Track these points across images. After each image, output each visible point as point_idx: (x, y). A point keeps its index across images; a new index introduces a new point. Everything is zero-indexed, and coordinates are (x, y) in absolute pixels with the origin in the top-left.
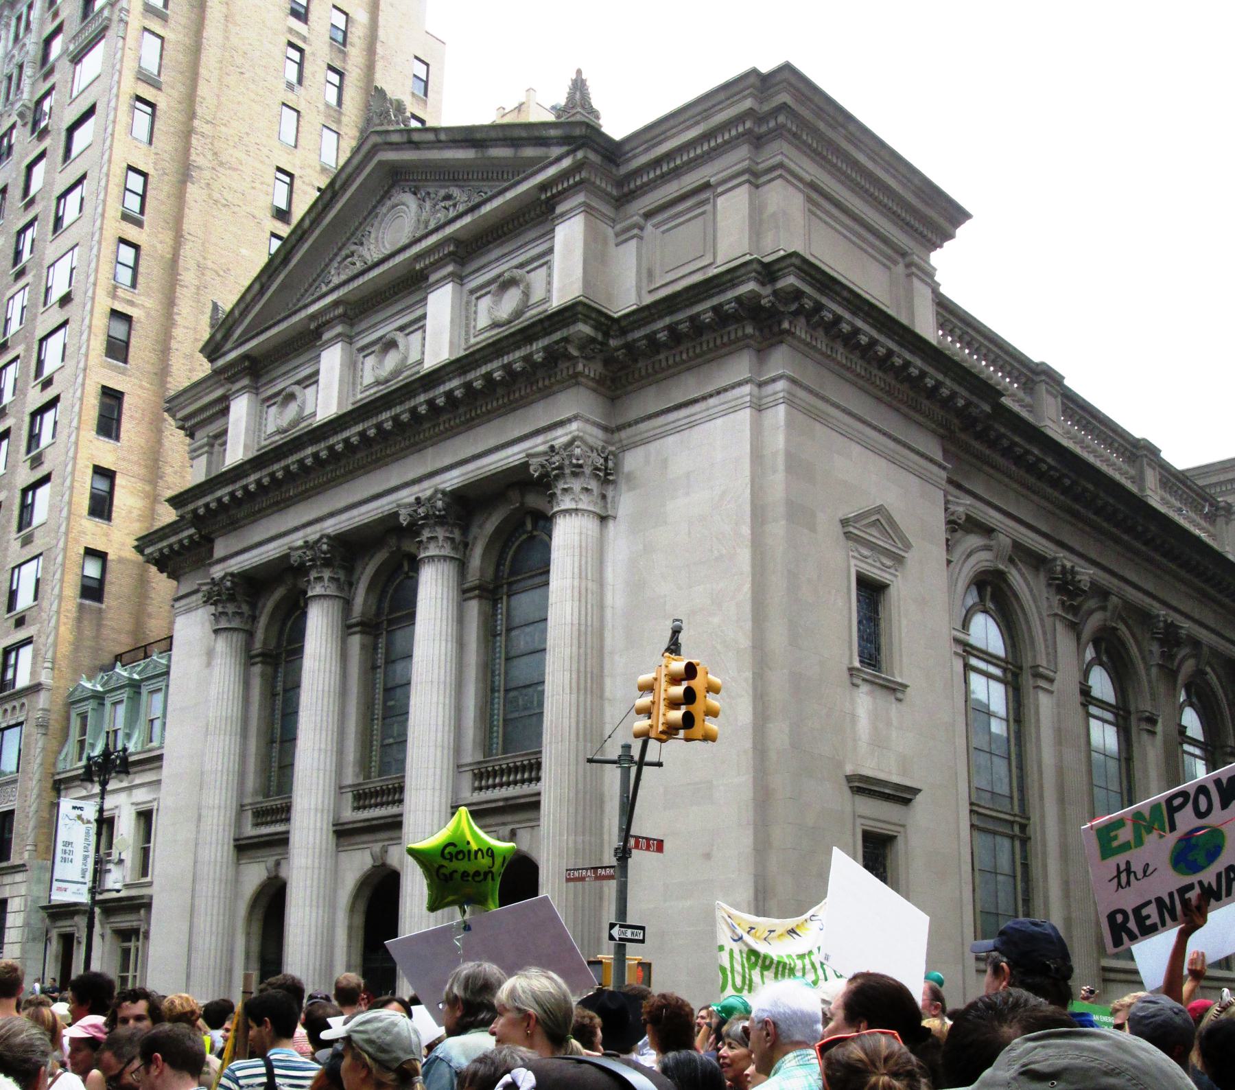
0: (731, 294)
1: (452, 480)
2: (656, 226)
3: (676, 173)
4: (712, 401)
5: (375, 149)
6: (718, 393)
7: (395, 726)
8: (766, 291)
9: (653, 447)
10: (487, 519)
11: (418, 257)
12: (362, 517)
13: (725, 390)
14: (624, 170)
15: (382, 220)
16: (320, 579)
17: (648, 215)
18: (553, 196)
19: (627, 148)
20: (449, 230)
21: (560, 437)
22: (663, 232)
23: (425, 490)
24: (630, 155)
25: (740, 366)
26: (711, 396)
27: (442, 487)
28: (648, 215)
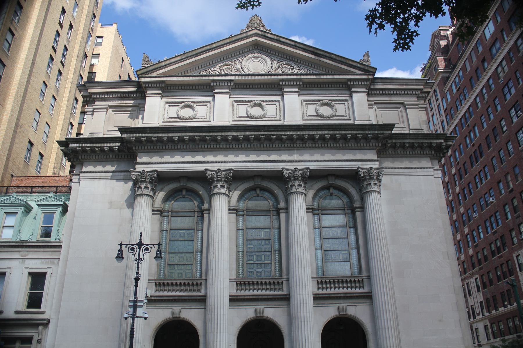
0: (435, 141)
1: (313, 166)
2: (378, 108)
3: (390, 95)
4: (418, 170)
5: (256, 35)
6: (421, 168)
7: (255, 256)
8: (444, 144)
9: (393, 177)
10: (315, 184)
11: (282, 80)
12: (253, 167)
13: (424, 168)
14: (372, 87)
15: (249, 60)
16: (222, 186)
17: (376, 103)
18: (353, 84)
19: (376, 81)
20: (302, 77)
21: (369, 165)
22: (380, 111)
23: (301, 166)
24: (376, 83)
25: (426, 162)
26: (418, 168)
27: (310, 167)
28: (376, 103)
